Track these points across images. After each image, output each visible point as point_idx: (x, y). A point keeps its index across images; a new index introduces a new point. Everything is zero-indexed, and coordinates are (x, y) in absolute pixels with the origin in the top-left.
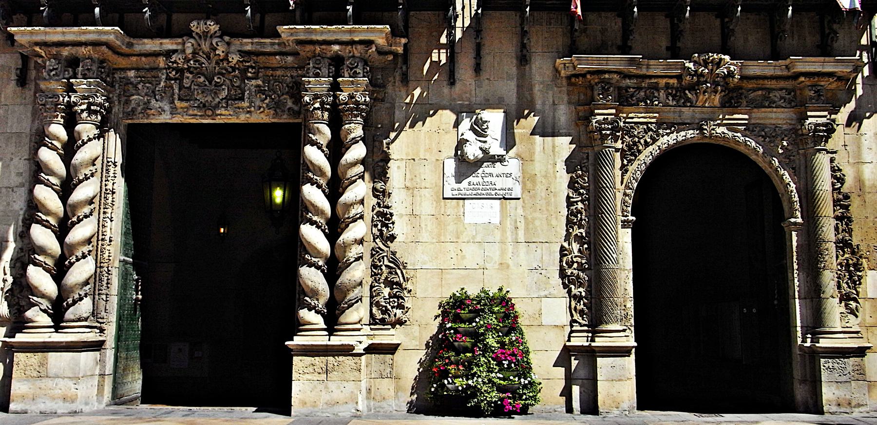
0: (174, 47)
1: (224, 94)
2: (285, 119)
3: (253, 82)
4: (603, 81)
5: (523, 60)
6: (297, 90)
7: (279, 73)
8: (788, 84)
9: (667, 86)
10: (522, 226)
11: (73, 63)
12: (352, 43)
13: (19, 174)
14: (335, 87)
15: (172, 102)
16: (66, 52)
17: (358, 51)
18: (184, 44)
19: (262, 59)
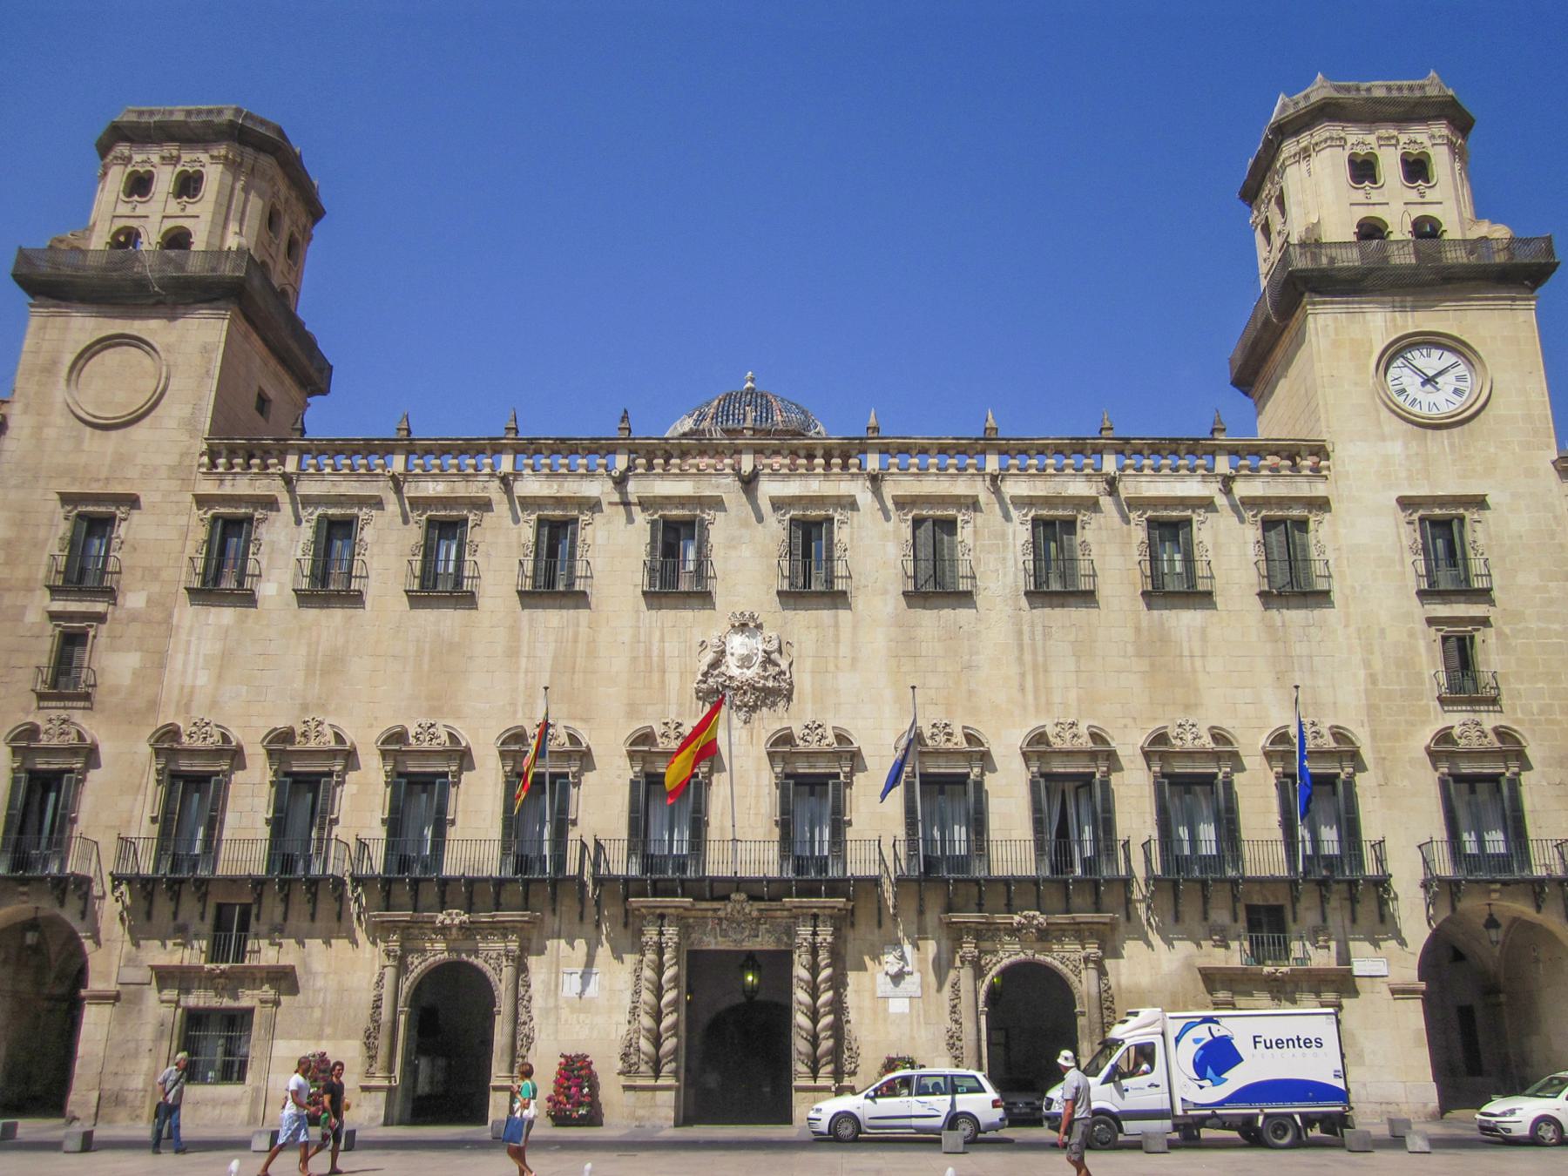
0: (719, 906)
1: (747, 933)
2: (783, 948)
3: (764, 926)
4: (967, 927)
5: (921, 912)
6: (790, 932)
7: (779, 920)
8: (1076, 927)
9: (1005, 929)
10: (922, 1013)
11: (662, 917)
12: (825, 907)
13: (626, 982)
14: (815, 934)
15: (716, 938)
16: (658, 911)
17: (828, 912)
18: (726, 905)
19: (770, 913)
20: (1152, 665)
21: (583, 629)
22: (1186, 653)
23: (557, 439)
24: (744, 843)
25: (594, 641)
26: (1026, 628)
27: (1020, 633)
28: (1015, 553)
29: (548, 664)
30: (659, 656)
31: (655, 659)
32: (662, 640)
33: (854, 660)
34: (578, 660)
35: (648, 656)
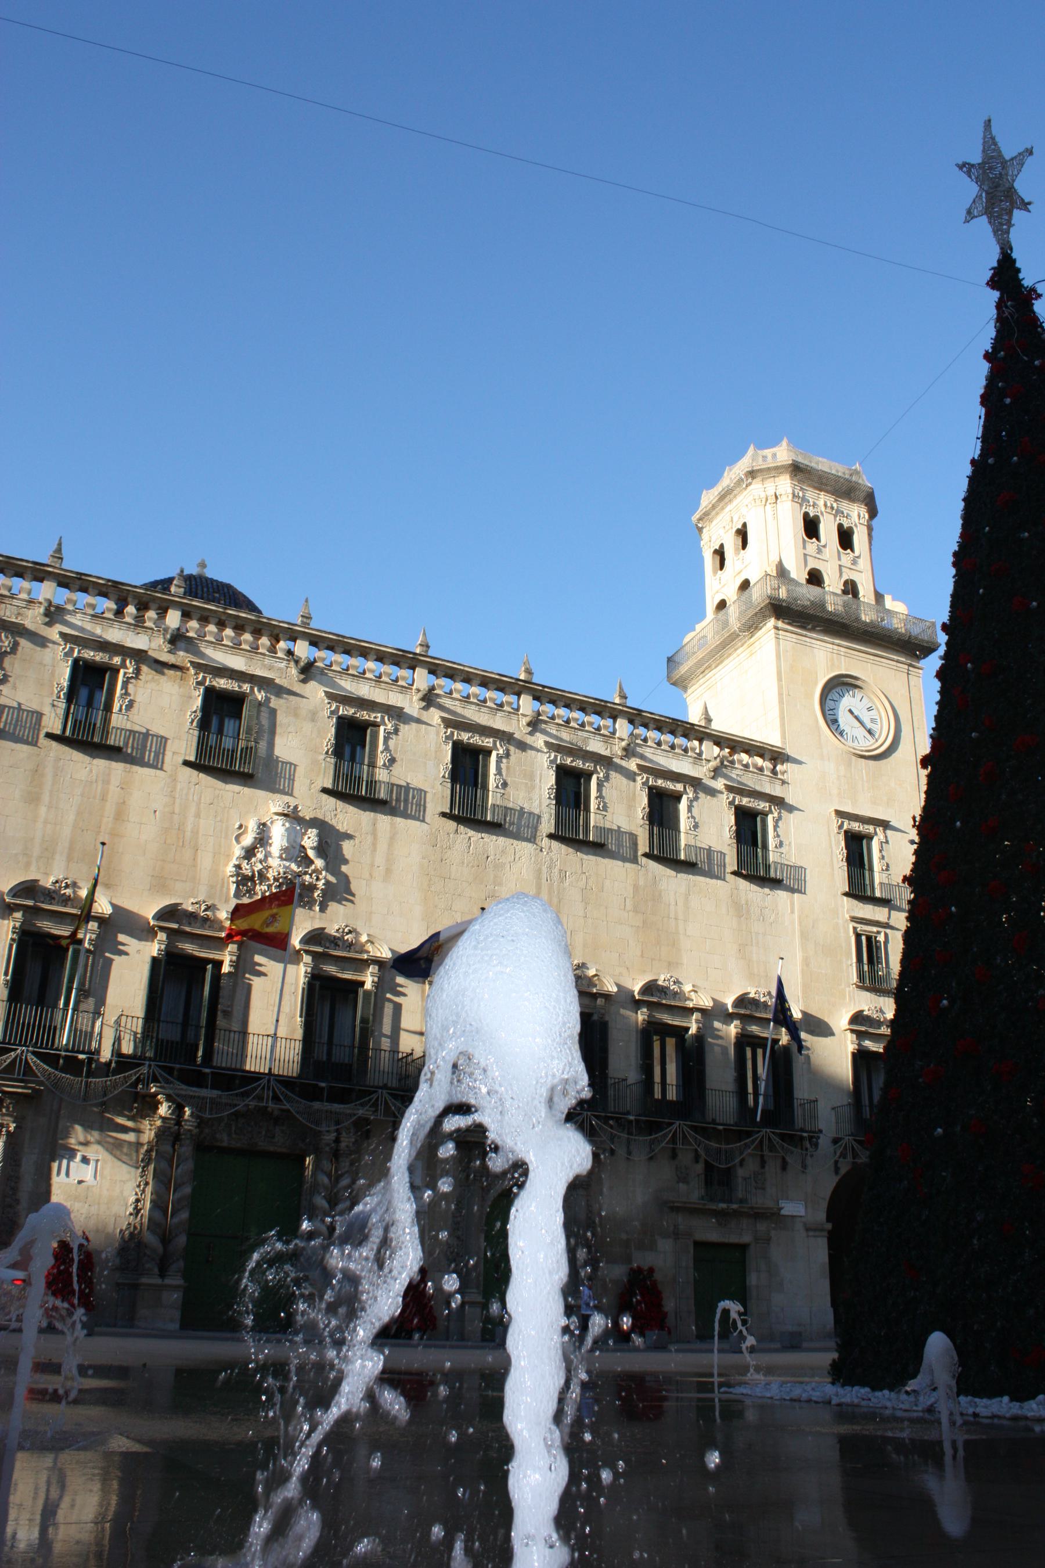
20: (644, 922)
21: (113, 788)
22: (672, 915)
23: (109, 581)
24: (265, 1038)
25: (124, 802)
26: (544, 869)
27: (539, 872)
28: (541, 795)
29: (71, 817)
30: (192, 832)
31: (188, 834)
32: (198, 815)
33: (388, 871)
34: (105, 820)
35: (181, 829)
